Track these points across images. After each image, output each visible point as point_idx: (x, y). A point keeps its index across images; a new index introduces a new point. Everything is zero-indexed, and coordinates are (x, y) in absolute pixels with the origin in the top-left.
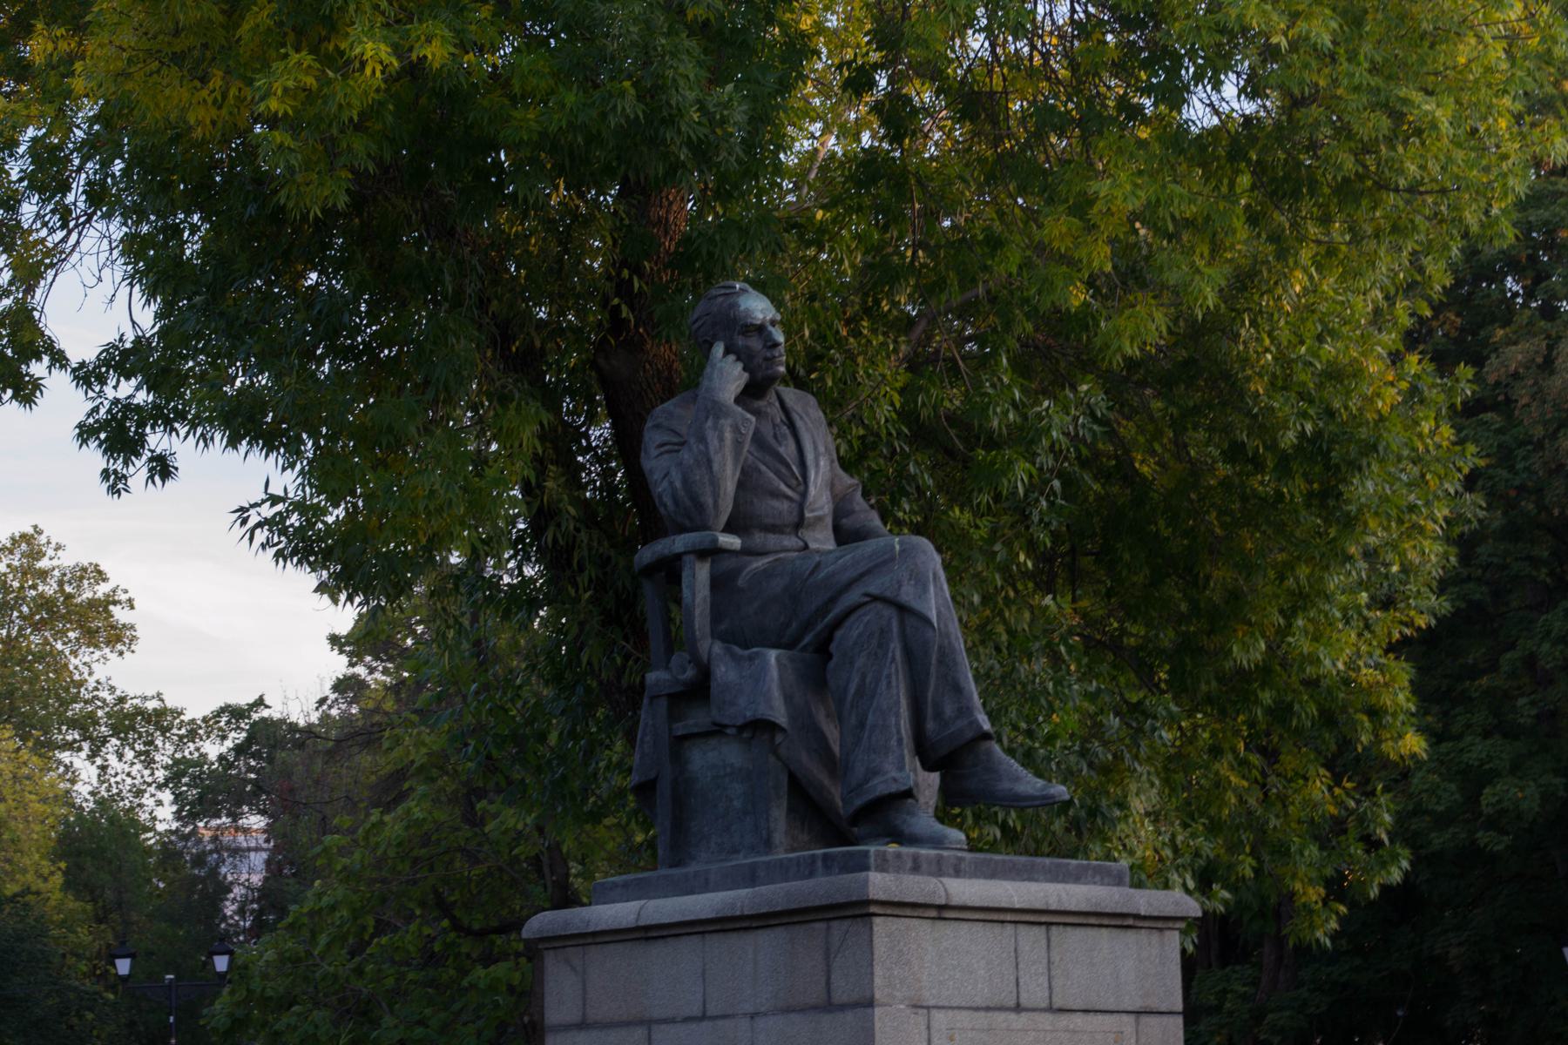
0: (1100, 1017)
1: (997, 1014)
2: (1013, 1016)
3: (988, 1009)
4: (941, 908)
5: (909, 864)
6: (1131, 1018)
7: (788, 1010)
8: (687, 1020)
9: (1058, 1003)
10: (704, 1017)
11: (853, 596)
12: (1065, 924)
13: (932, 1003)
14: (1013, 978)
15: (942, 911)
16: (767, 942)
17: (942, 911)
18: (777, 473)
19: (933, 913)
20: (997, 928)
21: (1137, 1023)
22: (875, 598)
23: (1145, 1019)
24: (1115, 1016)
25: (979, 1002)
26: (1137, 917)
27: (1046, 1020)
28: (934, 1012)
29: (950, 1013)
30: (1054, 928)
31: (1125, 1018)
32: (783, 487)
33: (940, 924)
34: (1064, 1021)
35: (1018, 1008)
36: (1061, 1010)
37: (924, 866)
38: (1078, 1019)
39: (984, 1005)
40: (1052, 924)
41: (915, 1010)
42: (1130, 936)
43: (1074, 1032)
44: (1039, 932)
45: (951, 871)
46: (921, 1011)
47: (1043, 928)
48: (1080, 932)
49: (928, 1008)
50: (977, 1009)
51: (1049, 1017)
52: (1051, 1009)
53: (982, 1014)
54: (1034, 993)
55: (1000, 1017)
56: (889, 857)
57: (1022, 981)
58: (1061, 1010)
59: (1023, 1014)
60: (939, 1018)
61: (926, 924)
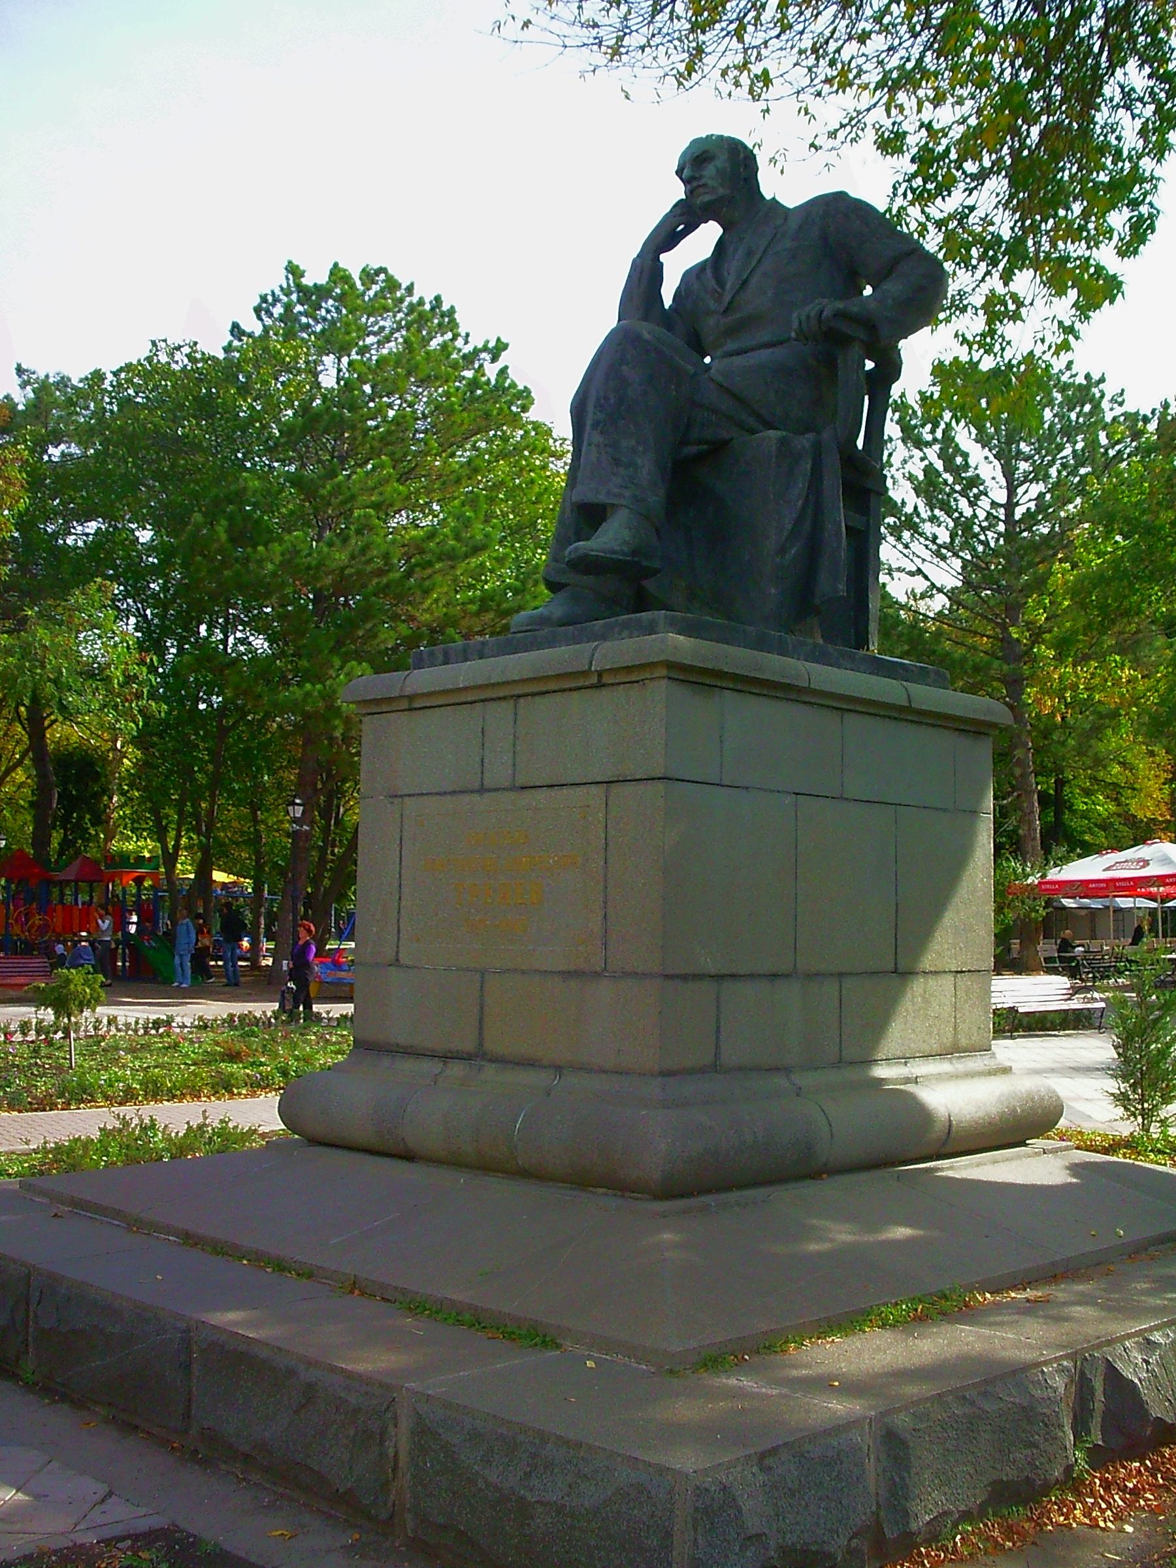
2: (476, 798)
5: (441, 657)
9: (520, 781)
12: (534, 695)
14: (478, 759)
23: (615, 789)
24: (584, 789)
30: (522, 701)
31: (594, 789)
35: (482, 790)
38: (540, 796)
39: (450, 789)
40: (519, 696)
41: (391, 800)
45: (476, 657)
46: (396, 801)
48: (547, 699)
49: (401, 796)
51: (512, 795)
52: (513, 788)
53: (449, 797)
57: (486, 760)
59: (487, 795)
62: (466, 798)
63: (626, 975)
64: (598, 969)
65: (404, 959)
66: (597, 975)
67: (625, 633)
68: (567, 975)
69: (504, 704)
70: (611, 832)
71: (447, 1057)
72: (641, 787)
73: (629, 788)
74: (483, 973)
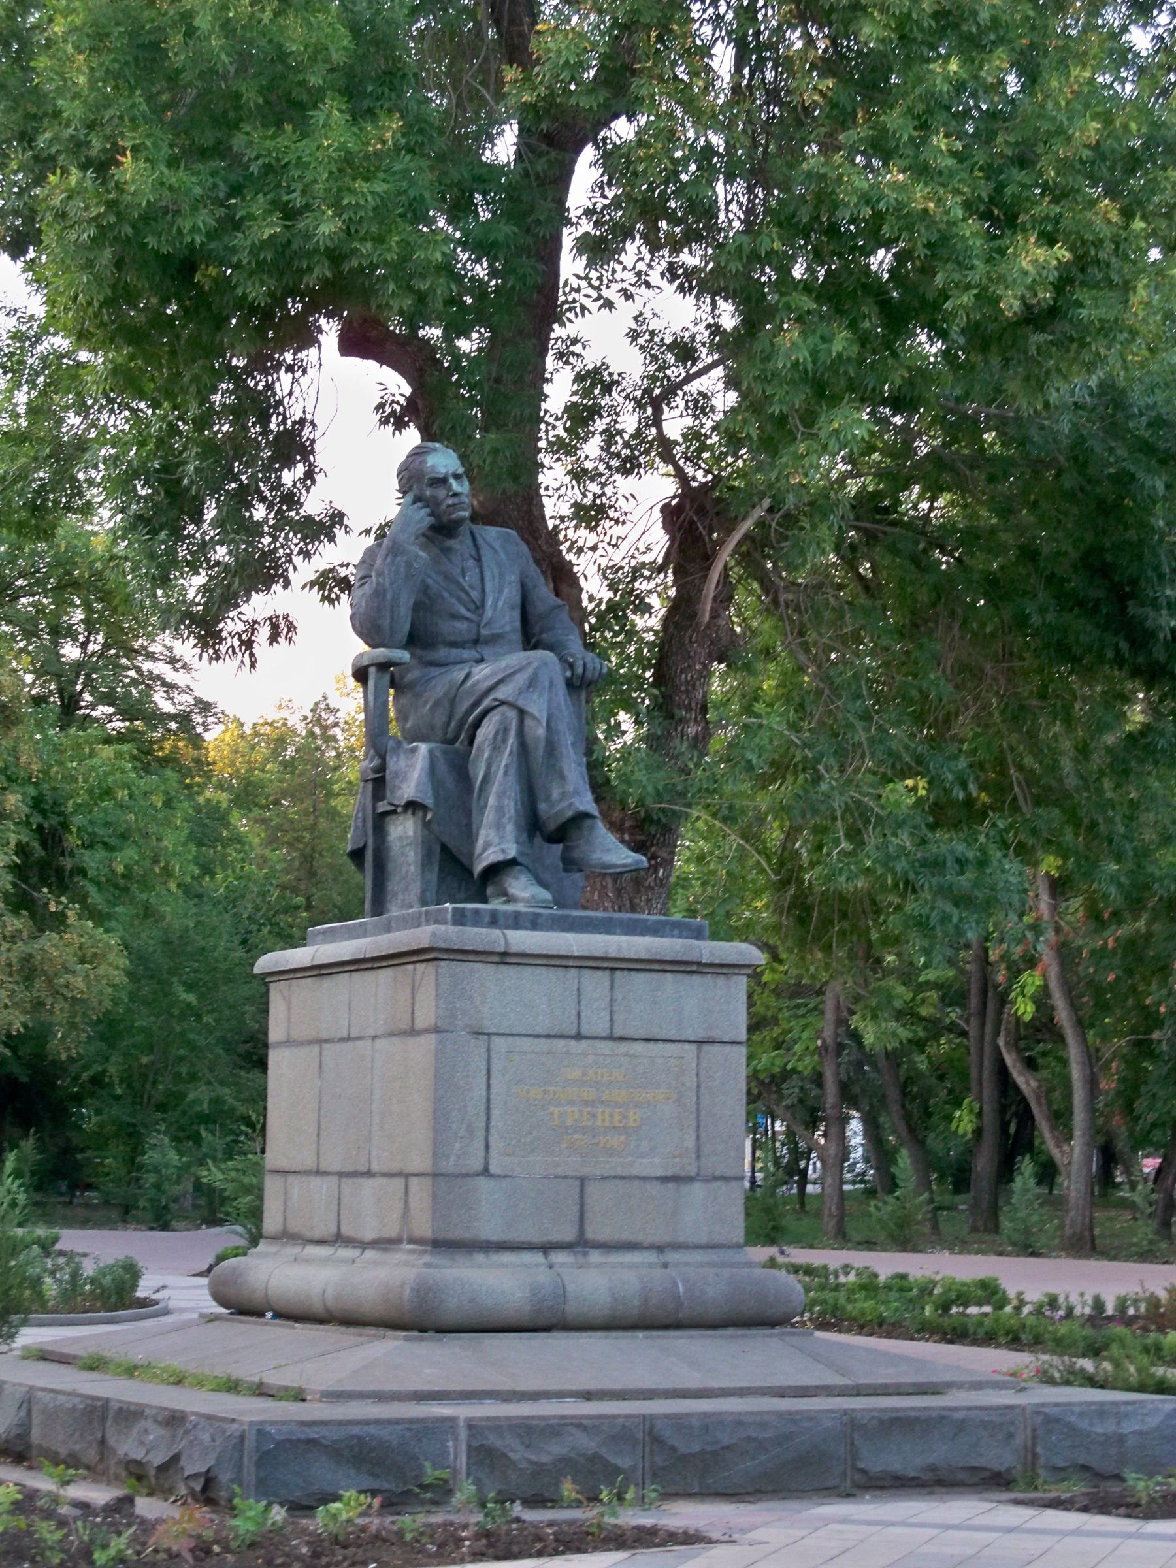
0: (661, 1045)
1: (555, 1041)
2: (573, 1043)
3: (548, 1036)
4: (504, 954)
5: (487, 919)
6: (693, 1047)
7: (392, 1034)
8: (342, 1040)
9: (618, 1032)
10: (348, 1039)
11: (486, 703)
12: (630, 970)
13: (493, 1030)
14: (574, 1012)
15: (505, 958)
16: (385, 976)
17: (505, 958)
18: (459, 600)
19: (496, 959)
20: (560, 972)
21: (699, 1051)
22: (503, 703)
23: (706, 1047)
25: (539, 1030)
26: (699, 964)
27: (606, 1047)
28: (494, 1038)
29: (510, 1039)
30: (618, 973)
31: (687, 1046)
32: (463, 611)
33: (503, 968)
34: (624, 1047)
35: (579, 1036)
36: (622, 1039)
37: (502, 921)
38: (639, 1047)
42: (696, 979)
43: (634, 1056)
44: (603, 977)
47: (607, 973)
48: (642, 975)
49: (489, 1034)
50: (538, 1036)
51: (611, 1044)
52: (611, 1038)
53: (543, 1040)
54: (596, 1022)
55: (561, 1043)
56: (469, 914)
57: (583, 1015)
58: (622, 1039)
60: (497, 1042)
61: (490, 968)
62: (562, 1042)
63: (716, 1178)
64: (692, 1174)
65: (493, 1169)
66: (690, 1179)
67: (676, 932)
68: (664, 1179)
69: (599, 973)
70: (703, 1078)
71: (546, 1248)
72: (728, 1048)
73: (715, 1048)
74: (583, 1181)
